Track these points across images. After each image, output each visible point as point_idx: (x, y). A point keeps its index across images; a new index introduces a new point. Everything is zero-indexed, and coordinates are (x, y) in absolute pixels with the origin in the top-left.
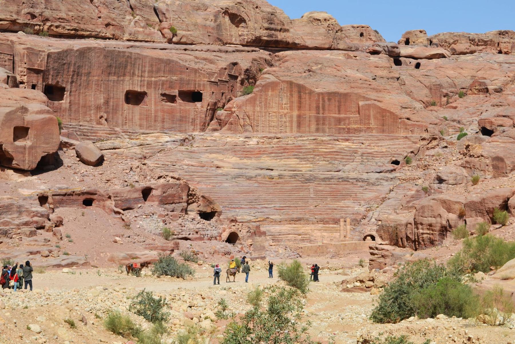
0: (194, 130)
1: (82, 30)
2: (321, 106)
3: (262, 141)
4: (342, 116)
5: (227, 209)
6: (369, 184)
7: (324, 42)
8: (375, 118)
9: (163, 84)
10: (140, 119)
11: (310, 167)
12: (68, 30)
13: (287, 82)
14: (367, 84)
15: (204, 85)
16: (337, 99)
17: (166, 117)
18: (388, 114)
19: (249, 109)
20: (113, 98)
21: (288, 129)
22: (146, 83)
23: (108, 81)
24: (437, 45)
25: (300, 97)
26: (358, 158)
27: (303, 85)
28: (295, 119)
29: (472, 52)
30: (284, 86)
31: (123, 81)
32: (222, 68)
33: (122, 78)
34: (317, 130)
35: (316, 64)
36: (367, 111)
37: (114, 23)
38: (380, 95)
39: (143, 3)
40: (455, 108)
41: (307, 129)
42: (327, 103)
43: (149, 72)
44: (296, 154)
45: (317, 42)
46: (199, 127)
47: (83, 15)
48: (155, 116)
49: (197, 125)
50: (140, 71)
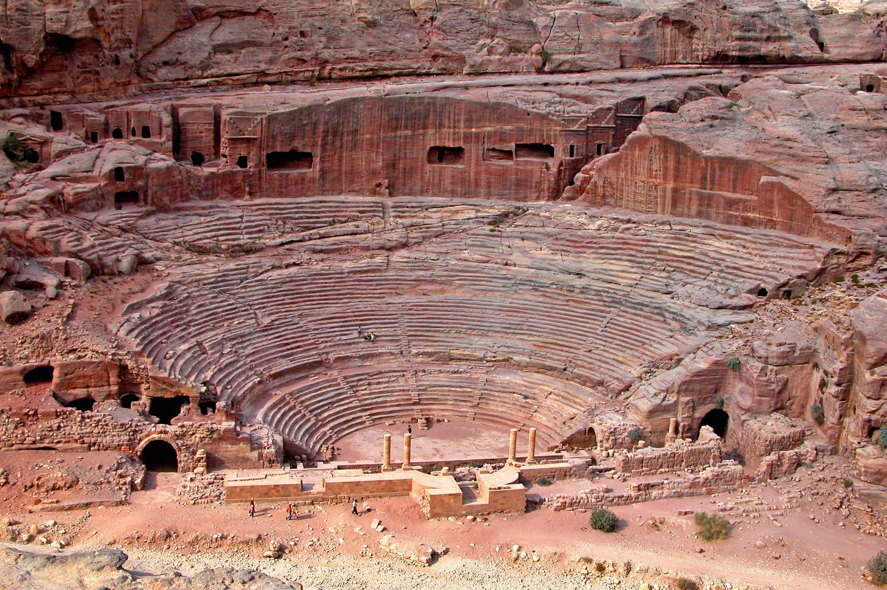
0: (538, 198)
1: (385, 69)
2: (708, 176)
4: (738, 196)
5: (462, 335)
7: (862, 51)
8: (781, 206)
9: (490, 138)
10: (452, 183)
11: (635, 279)
12: (360, 71)
14: (785, 146)
17: (493, 180)
18: (799, 202)
19: (611, 174)
20: (405, 158)
21: (659, 208)
23: (395, 137)
25: (678, 162)
27: (683, 143)
28: (669, 194)
30: (656, 143)
31: (424, 135)
33: (421, 131)
34: (699, 214)
36: (769, 193)
37: (445, 53)
39: (516, 19)
41: (686, 211)
42: (718, 173)
43: (466, 121)
44: (633, 253)
45: (850, 51)
46: (546, 194)
47: (393, 48)
48: (476, 180)
49: (544, 190)
50: (452, 121)
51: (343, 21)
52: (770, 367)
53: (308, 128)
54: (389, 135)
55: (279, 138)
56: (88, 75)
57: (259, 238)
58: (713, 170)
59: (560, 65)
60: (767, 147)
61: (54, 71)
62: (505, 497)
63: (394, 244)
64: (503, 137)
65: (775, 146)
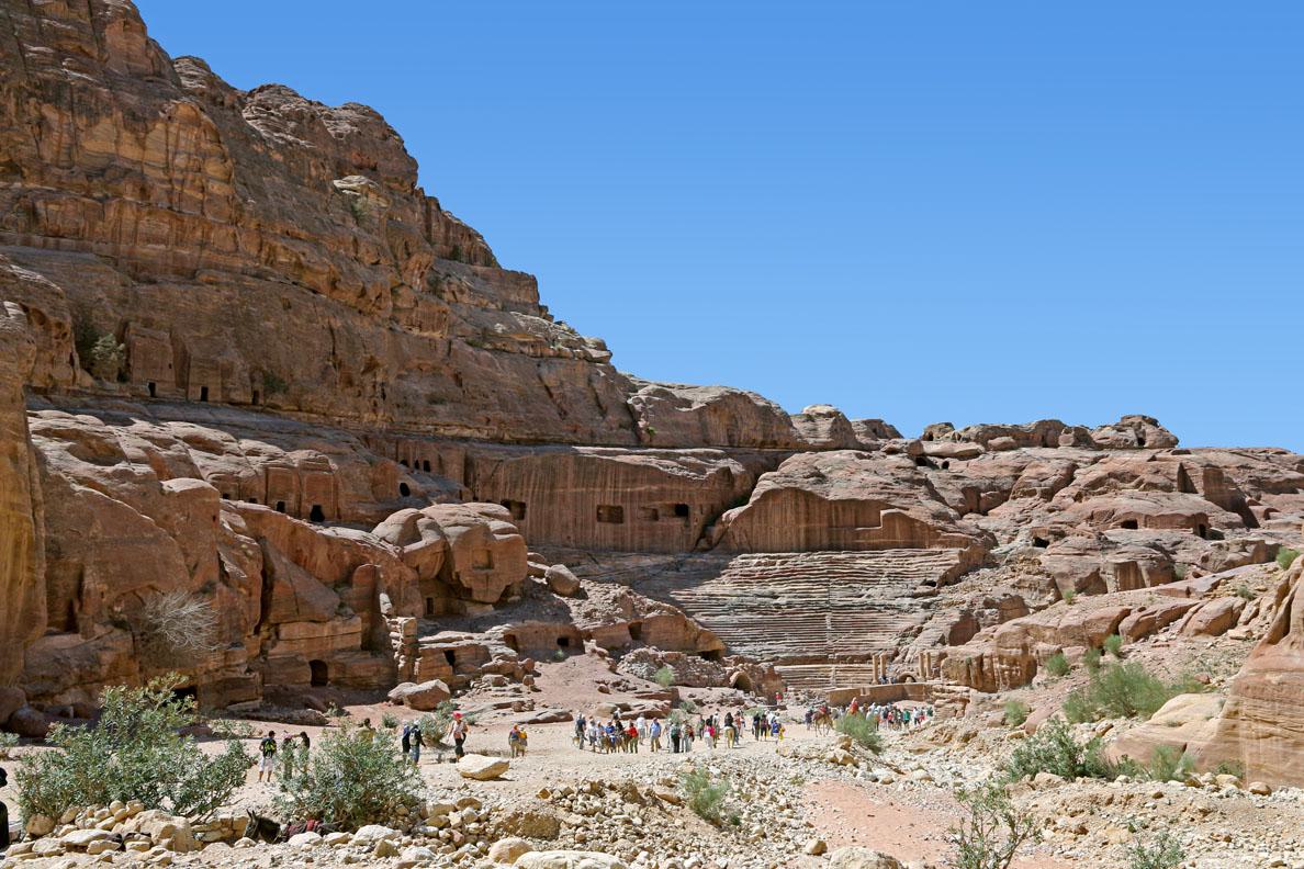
3: (763, 561)
6: (901, 611)
16: (853, 508)
24: (967, 440)
25: (807, 506)
26: (884, 579)
28: (802, 535)
29: (1012, 448)
35: (826, 466)
38: (907, 501)
40: (998, 515)
43: (624, 481)
58: (836, 508)
60: (878, 489)
65: (882, 488)
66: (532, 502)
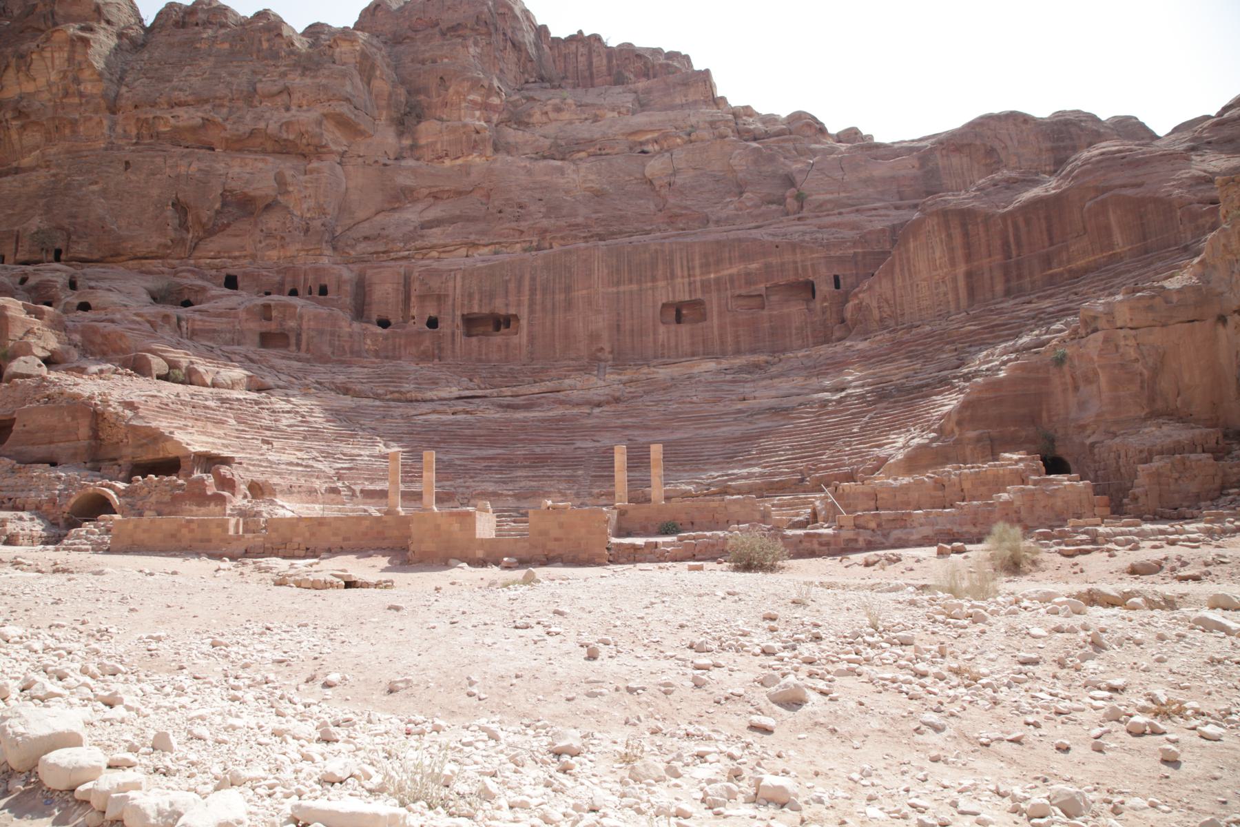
2: (1012, 239)
10: (693, 344)
13: (936, 213)
15: (813, 265)
22: (698, 285)
23: (618, 293)
25: (966, 234)
27: (968, 209)
28: (961, 283)
31: (653, 289)
32: (870, 232)
33: (649, 284)
34: (1008, 293)
43: (701, 266)
50: (685, 269)
51: (567, 192)
52: (1122, 332)
53: (512, 286)
54: (610, 290)
55: (477, 297)
56: (273, 241)
57: (431, 390)
58: (1016, 228)
59: (821, 205)
61: (236, 236)
62: (561, 525)
63: (602, 398)
64: (749, 278)
66: (532, 311)
